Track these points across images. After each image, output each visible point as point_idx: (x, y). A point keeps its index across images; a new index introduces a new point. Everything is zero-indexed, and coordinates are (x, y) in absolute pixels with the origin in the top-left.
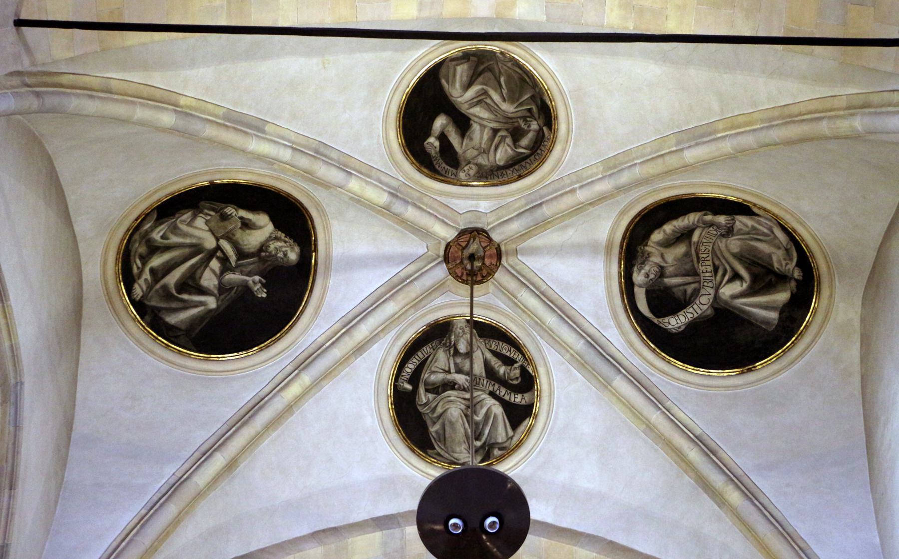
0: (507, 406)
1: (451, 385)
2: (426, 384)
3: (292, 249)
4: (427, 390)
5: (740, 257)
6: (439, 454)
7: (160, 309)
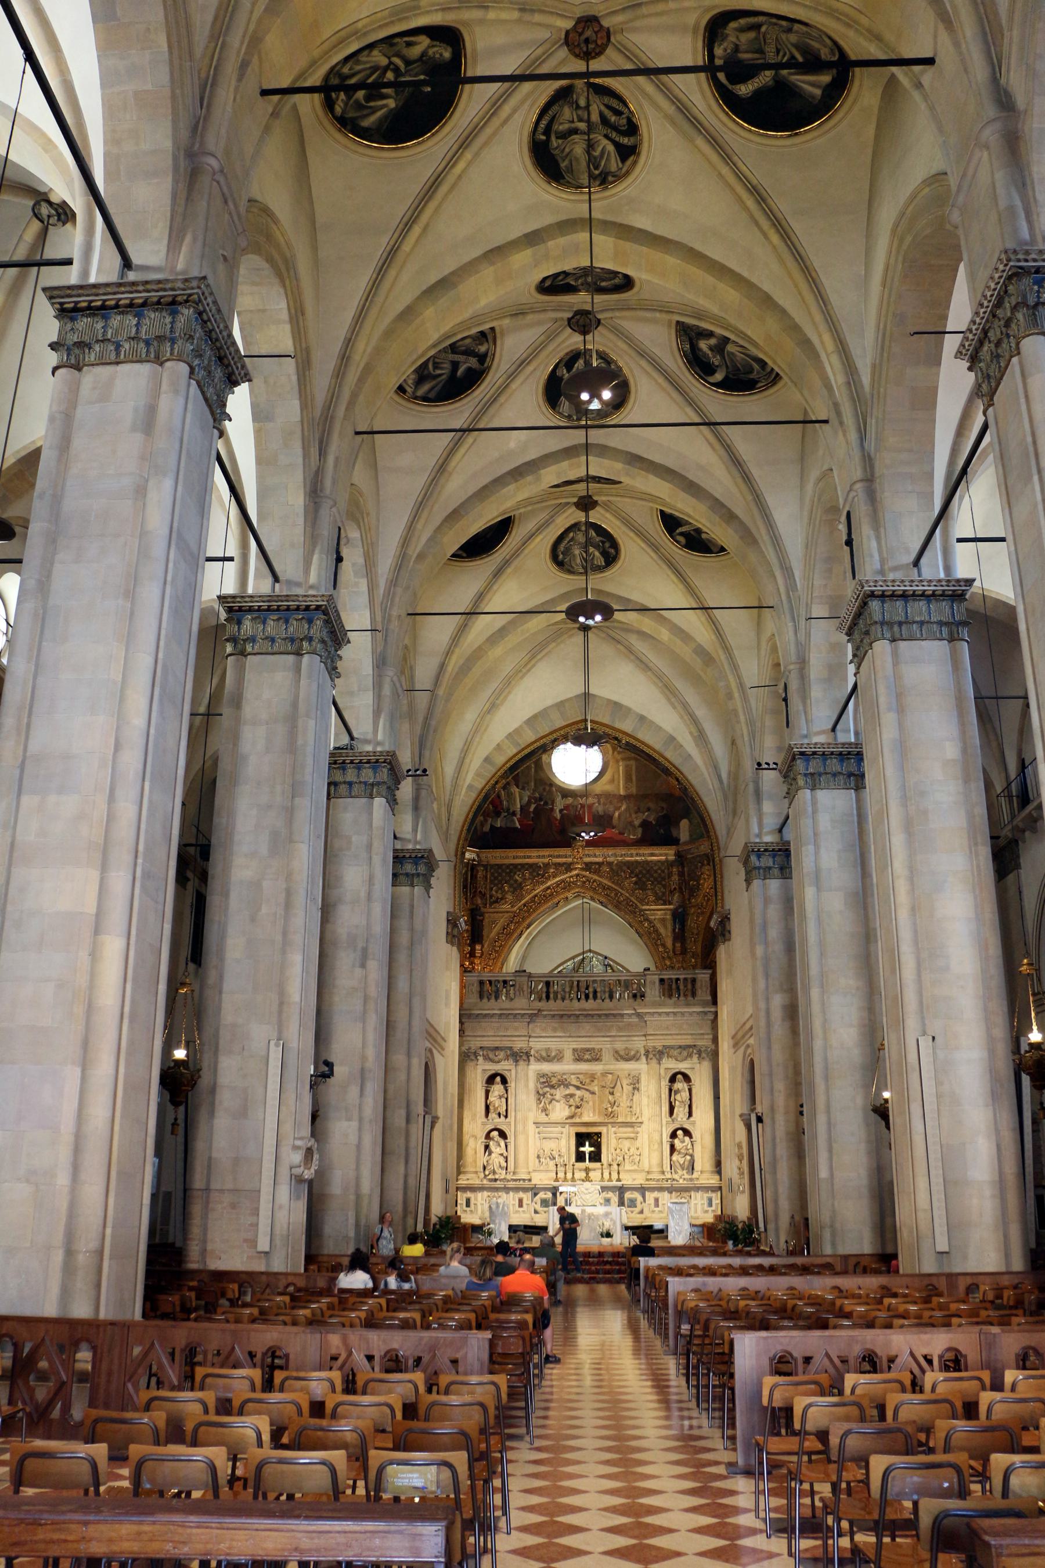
0: (617, 145)
1: (575, 131)
2: (556, 133)
3: (446, 50)
4: (557, 138)
5: (797, 46)
6: (568, 182)
7: (356, 118)
